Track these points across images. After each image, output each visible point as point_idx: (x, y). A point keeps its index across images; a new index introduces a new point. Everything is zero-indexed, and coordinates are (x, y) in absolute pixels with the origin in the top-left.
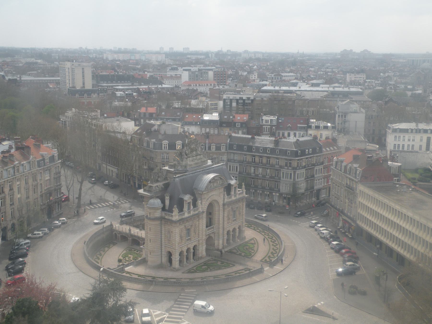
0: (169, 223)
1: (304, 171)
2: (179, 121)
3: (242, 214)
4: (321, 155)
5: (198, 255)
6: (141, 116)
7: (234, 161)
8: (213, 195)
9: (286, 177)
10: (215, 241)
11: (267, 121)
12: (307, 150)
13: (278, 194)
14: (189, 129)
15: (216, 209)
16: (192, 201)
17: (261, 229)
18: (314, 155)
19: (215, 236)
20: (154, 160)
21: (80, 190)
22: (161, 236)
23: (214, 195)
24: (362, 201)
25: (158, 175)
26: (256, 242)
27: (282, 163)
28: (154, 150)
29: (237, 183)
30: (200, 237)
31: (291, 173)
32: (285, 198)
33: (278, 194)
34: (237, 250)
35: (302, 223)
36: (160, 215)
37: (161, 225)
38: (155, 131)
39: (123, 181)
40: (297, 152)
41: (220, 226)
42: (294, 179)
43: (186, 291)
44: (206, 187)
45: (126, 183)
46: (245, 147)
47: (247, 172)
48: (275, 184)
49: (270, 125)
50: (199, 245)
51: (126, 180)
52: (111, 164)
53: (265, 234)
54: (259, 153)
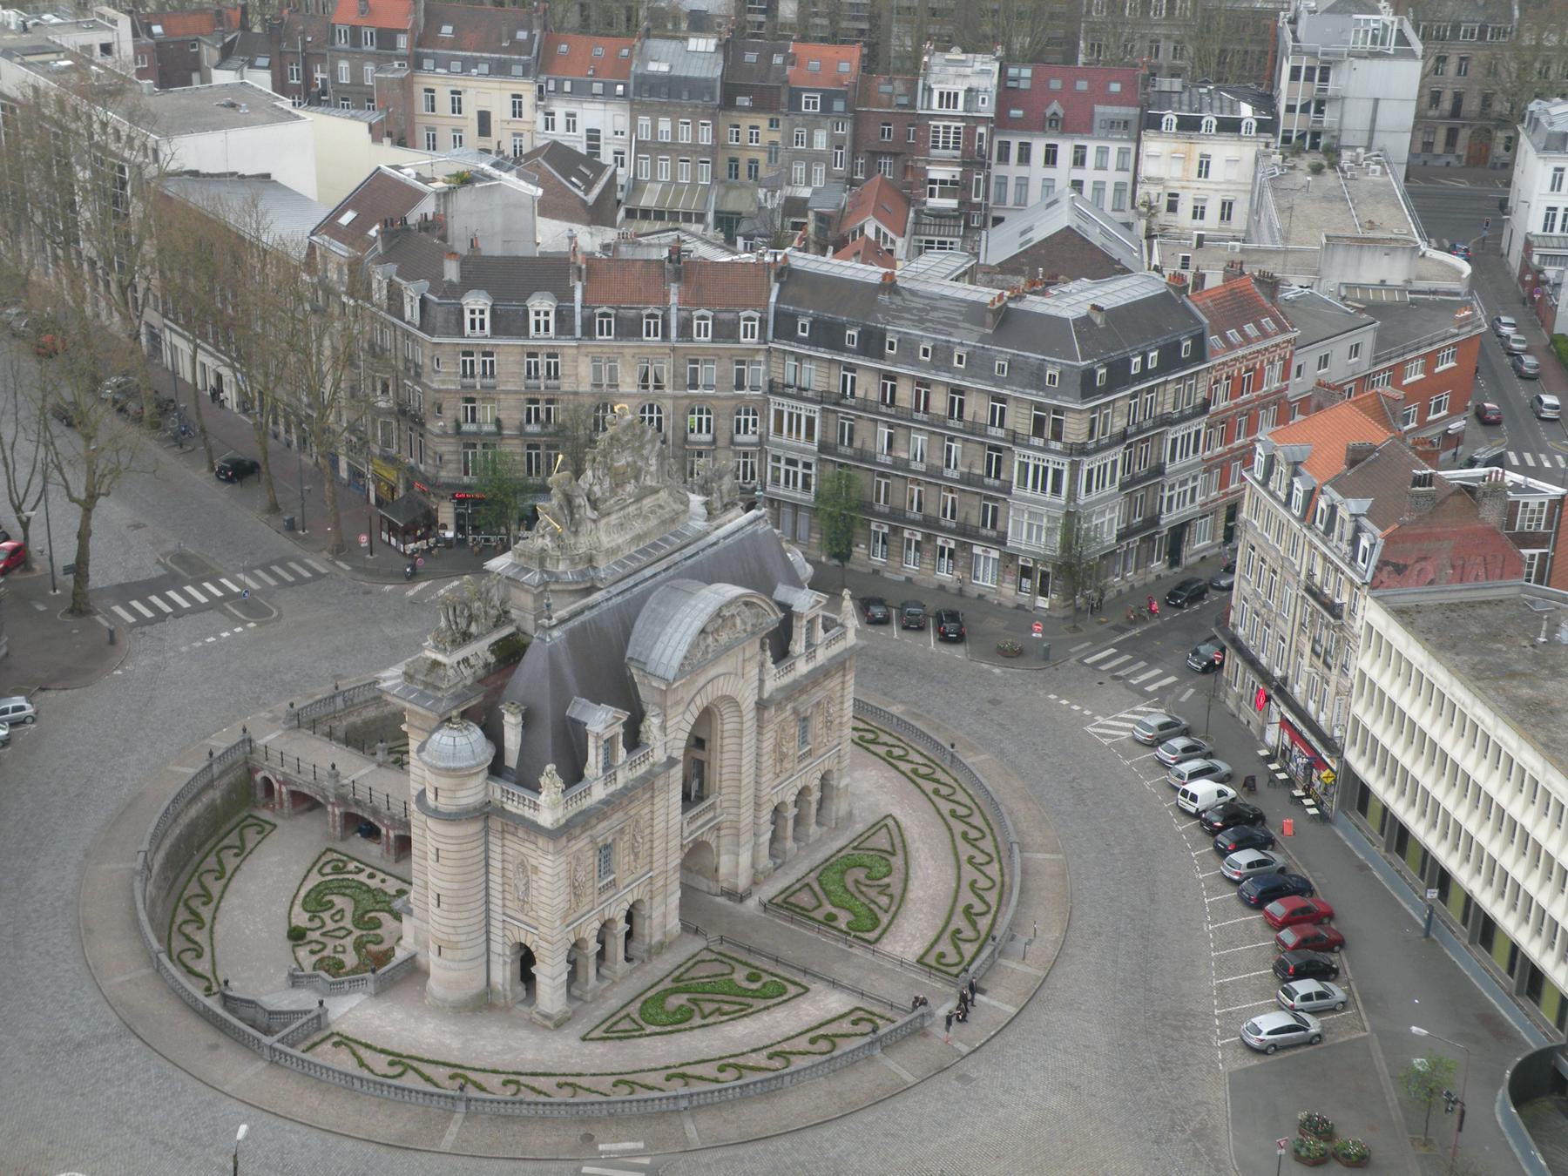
0: (521, 833)
1: (1117, 454)
2: (525, 74)
3: (838, 721)
4: (1198, 372)
5: (647, 940)
6: (338, 46)
7: (800, 394)
8: (712, 680)
9: (1035, 486)
10: (719, 856)
11: (949, 99)
12: (1135, 360)
13: (995, 554)
14: (574, 115)
15: (726, 727)
16: (621, 730)
17: (920, 760)
18: (1170, 378)
19: (718, 837)
20: (424, 380)
21: (84, 536)
22: (487, 880)
23: (718, 676)
24: (1373, 673)
25: (470, 608)
26: (897, 841)
27: (1018, 419)
28: (421, 334)
29: (819, 602)
30: (655, 865)
31: (1060, 467)
32: (1026, 572)
33: (995, 554)
34: (815, 894)
35: (1100, 719)
36: (481, 796)
37: (487, 834)
38: (427, 225)
39: (276, 436)
40: (1089, 375)
41: (743, 796)
42: (1072, 496)
43: (602, 1153)
44: (686, 658)
45: (289, 445)
46: (854, 332)
47: (857, 444)
48: (986, 507)
49: (962, 119)
50: (651, 898)
51: (288, 431)
52: (209, 344)
53: (936, 792)
54: (915, 363)
